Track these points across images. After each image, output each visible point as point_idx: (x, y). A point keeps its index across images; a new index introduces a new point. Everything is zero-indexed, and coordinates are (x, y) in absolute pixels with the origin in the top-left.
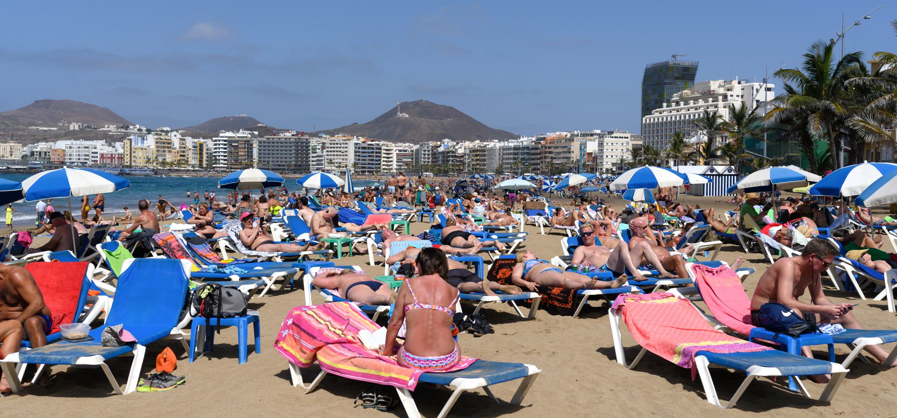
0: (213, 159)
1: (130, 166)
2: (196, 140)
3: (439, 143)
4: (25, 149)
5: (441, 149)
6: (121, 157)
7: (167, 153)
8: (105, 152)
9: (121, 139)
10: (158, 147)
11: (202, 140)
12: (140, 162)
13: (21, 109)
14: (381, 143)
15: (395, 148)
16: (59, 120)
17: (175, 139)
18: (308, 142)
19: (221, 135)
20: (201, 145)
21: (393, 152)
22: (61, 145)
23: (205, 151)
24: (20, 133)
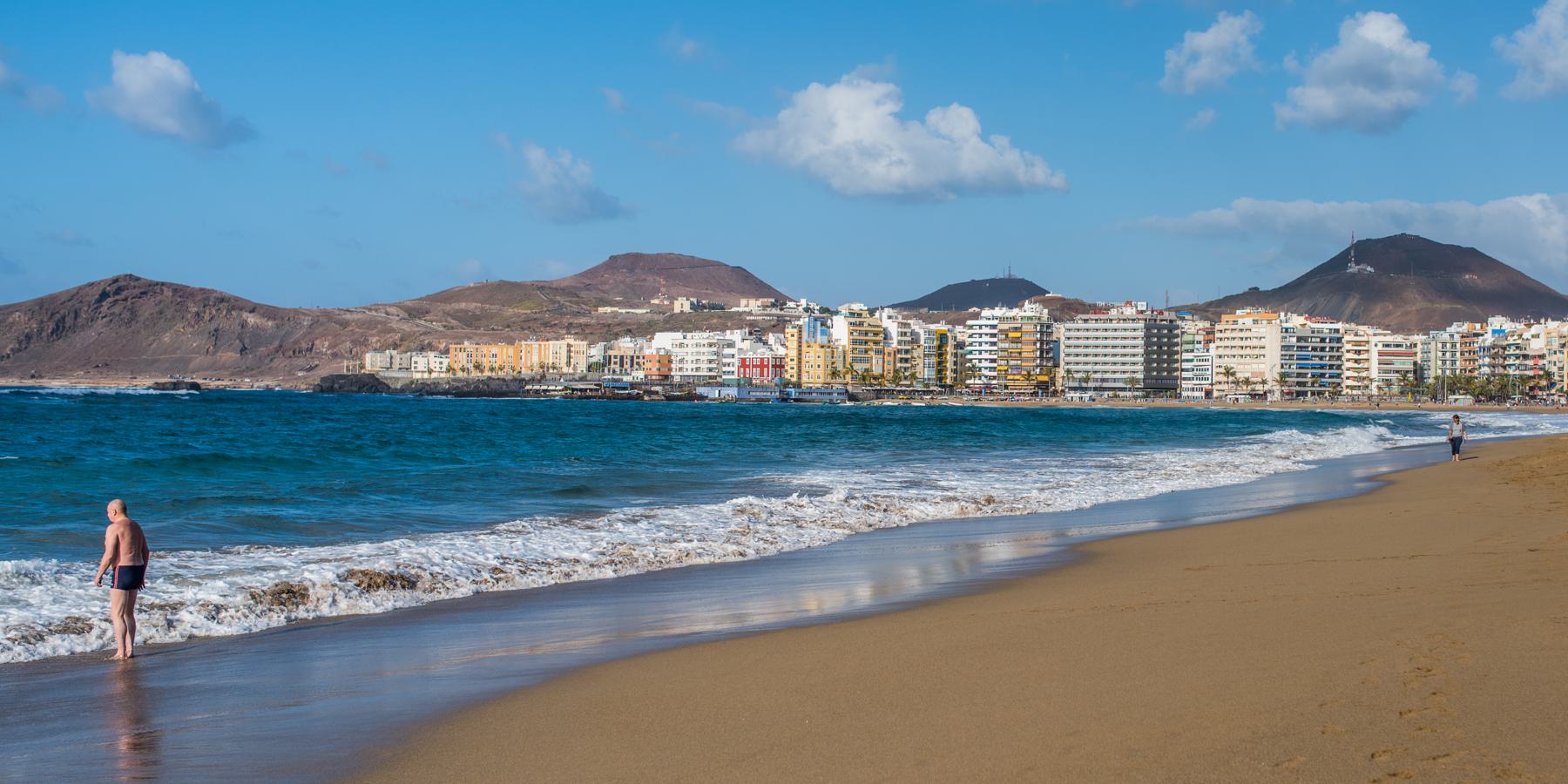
0: (965, 370)
1: (798, 385)
2: (933, 327)
3: (1478, 326)
4: (593, 351)
5: (1489, 339)
6: (779, 365)
7: (872, 353)
8: (750, 355)
9: (779, 325)
10: (854, 342)
11: (942, 327)
12: (814, 376)
13: (583, 275)
14: (1339, 326)
15: (1375, 339)
16: (654, 293)
17: (889, 322)
18: (1172, 326)
19: (986, 312)
20: (943, 337)
21: (1370, 351)
22: (664, 341)
23: (950, 349)
24: (582, 320)
